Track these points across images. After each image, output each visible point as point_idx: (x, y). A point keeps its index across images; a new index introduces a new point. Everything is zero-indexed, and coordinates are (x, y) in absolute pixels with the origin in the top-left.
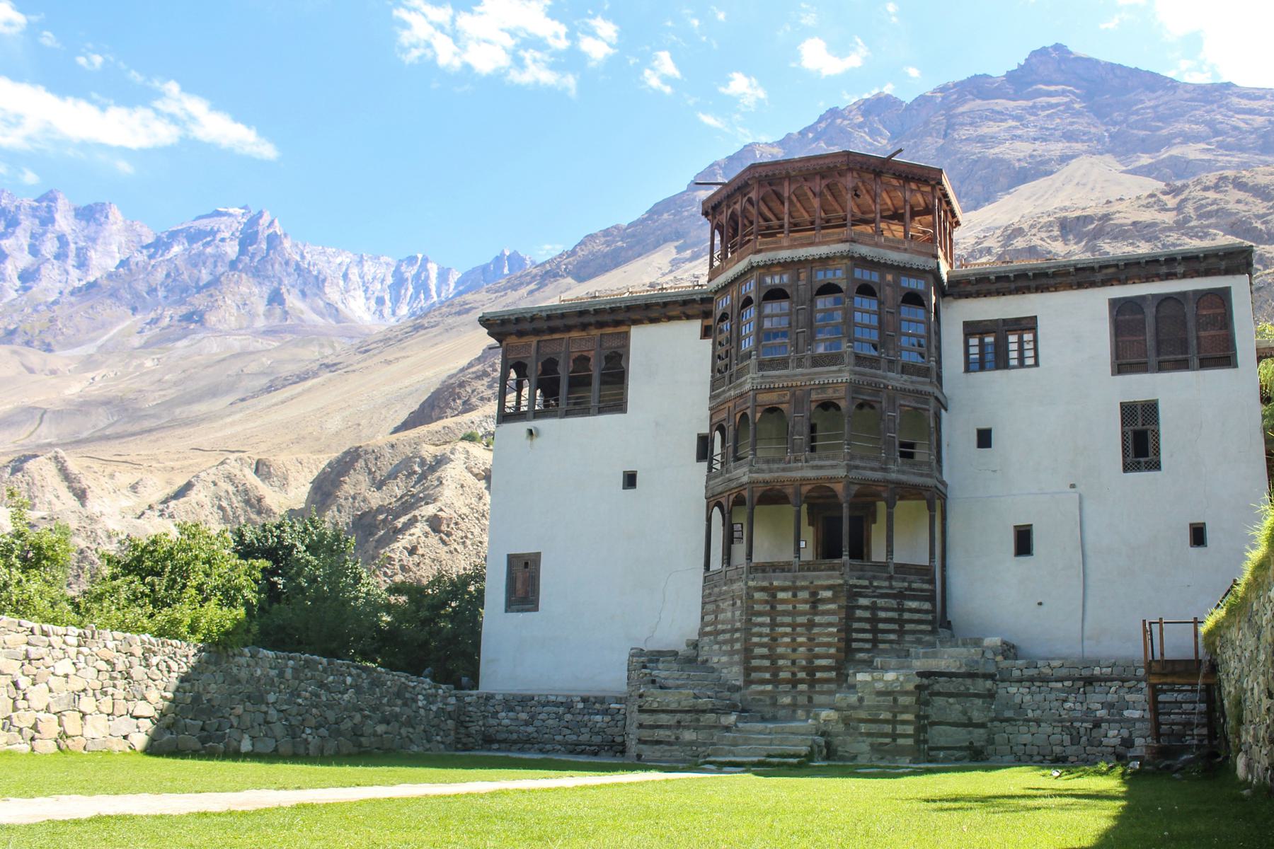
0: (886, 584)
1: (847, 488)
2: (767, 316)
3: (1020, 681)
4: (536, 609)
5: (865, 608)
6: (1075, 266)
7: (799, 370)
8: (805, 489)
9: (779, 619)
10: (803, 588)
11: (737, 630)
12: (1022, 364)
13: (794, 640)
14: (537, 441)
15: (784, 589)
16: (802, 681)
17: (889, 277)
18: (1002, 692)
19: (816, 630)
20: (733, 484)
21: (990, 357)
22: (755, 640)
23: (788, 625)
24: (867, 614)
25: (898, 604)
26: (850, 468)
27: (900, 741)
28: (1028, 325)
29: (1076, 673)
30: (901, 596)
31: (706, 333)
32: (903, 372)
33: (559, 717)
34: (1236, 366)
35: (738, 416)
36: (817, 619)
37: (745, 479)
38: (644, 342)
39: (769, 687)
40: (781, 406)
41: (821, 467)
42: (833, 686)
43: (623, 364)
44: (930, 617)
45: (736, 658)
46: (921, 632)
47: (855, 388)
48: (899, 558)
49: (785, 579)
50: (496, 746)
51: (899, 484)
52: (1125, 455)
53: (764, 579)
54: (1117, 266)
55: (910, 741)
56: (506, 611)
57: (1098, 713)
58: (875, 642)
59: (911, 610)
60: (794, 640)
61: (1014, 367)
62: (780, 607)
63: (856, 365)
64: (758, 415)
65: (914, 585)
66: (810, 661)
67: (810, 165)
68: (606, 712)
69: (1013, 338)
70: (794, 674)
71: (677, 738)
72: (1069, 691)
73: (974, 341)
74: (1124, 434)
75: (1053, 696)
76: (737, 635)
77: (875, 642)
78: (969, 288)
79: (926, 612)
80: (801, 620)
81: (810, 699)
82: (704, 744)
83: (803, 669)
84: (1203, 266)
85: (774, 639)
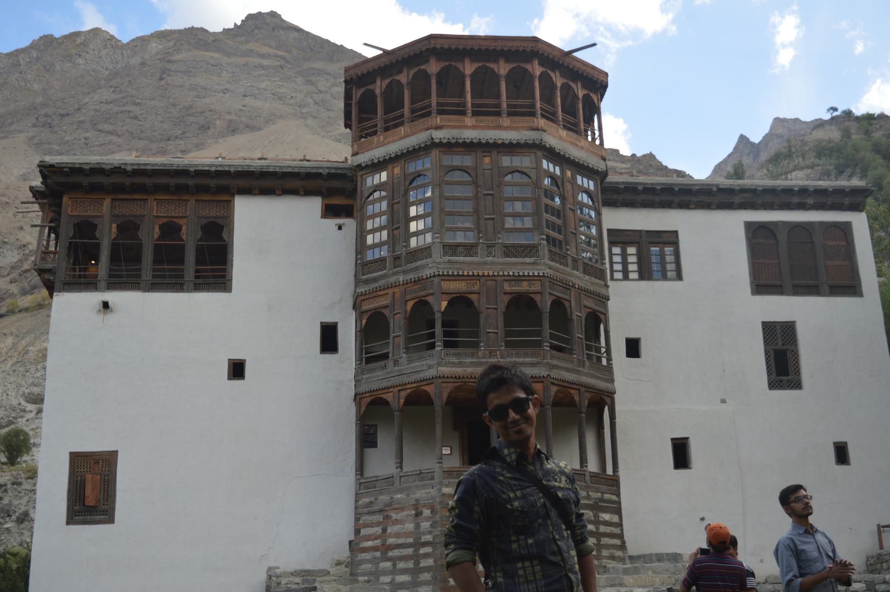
1: (546, 389)
2: (448, 199)
4: (111, 520)
6: (717, 186)
11: (425, 544)
12: (665, 278)
14: (111, 318)
20: (410, 379)
21: (633, 267)
25: (595, 516)
28: (670, 239)
31: (330, 211)
32: (584, 272)
34: (860, 295)
35: (410, 305)
37: (432, 373)
38: (250, 216)
40: (473, 297)
43: (225, 236)
44: (616, 531)
45: (426, 576)
46: (614, 546)
47: (553, 281)
51: (588, 387)
52: (769, 373)
56: (68, 523)
61: (657, 280)
64: (444, 304)
67: (499, 46)
69: (655, 249)
73: (616, 250)
74: (767, 352)
76: (428, 550)
78: (615, 197)
84: (829, 200)
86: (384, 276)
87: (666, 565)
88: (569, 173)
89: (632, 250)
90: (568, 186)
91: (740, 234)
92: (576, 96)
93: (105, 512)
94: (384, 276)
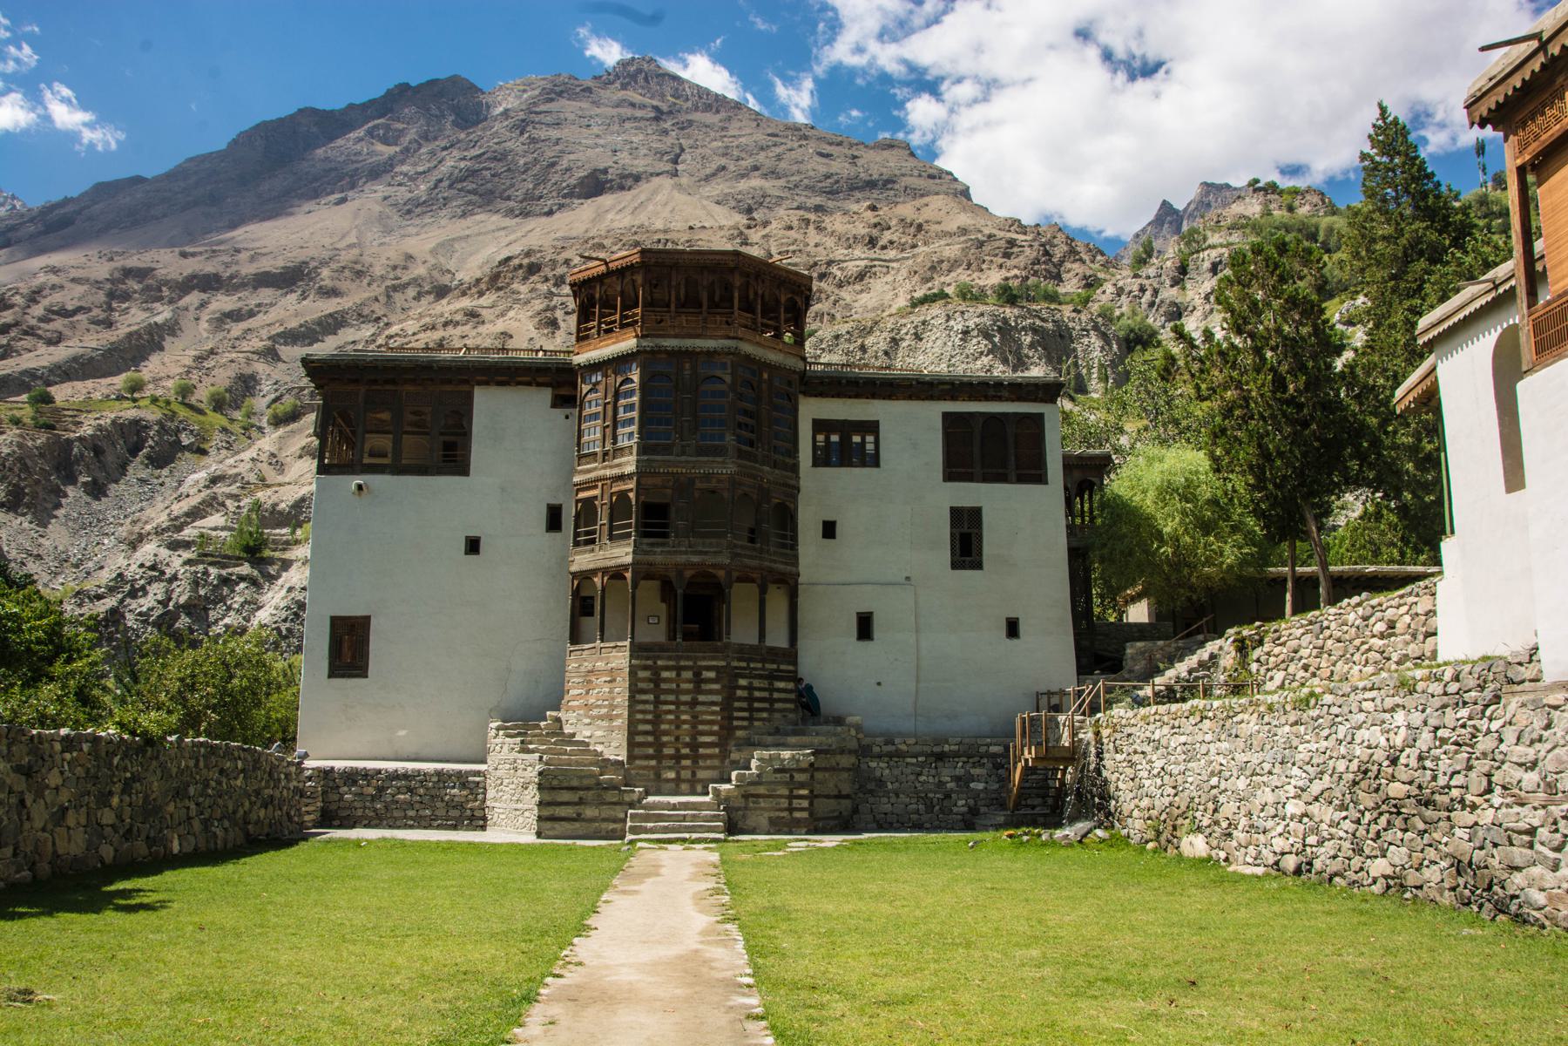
0: (759, 665)
3: (880, 756)
5: (743, 688)
7: (683, 458)
8: (688, 574)
9: (662, 697)
12: (863, 464)
13: (678, 717)
15: (667, 668)
18: (863, 766)
19: (699, 708)
22: (639, 716)
23: (671, 703)
27: (797, 815)
28: (872, 427)
29: (927, 749)
30: (772, 677)
33: (410, 790)
36: (701, 698)
38: (487, 404)
39: (653, 763)
41: (706, 553)
42: (716, 762)
48: (771, 641)
49: (669, 658)
50: (336, 823)
51: (771, 571)
53: (648, 658)
54: (952, 384)
55: (805, 815)
57: (949, 786)
59: (779, 690)
60: (678, 717)
63: (739, 457)
65: (783, 667)
66: (694, 738)
68: (464, 786)
70: (678, 750)
71: (579, 815)
72: (922, 765)
73: (820, 438)
75: (909, 771)
77: (750, 719)
79: (790, 691)
81: (694, 774)
82: (604, 820)
83: (687, 745)
86: (595, 469)
87: (830, 728)
88: (765, 376)
89: (835, 438)
90: (764, 386)
91: (938, 423)
92: (778, 301)
93: (360, 668)
94: (595, 469)
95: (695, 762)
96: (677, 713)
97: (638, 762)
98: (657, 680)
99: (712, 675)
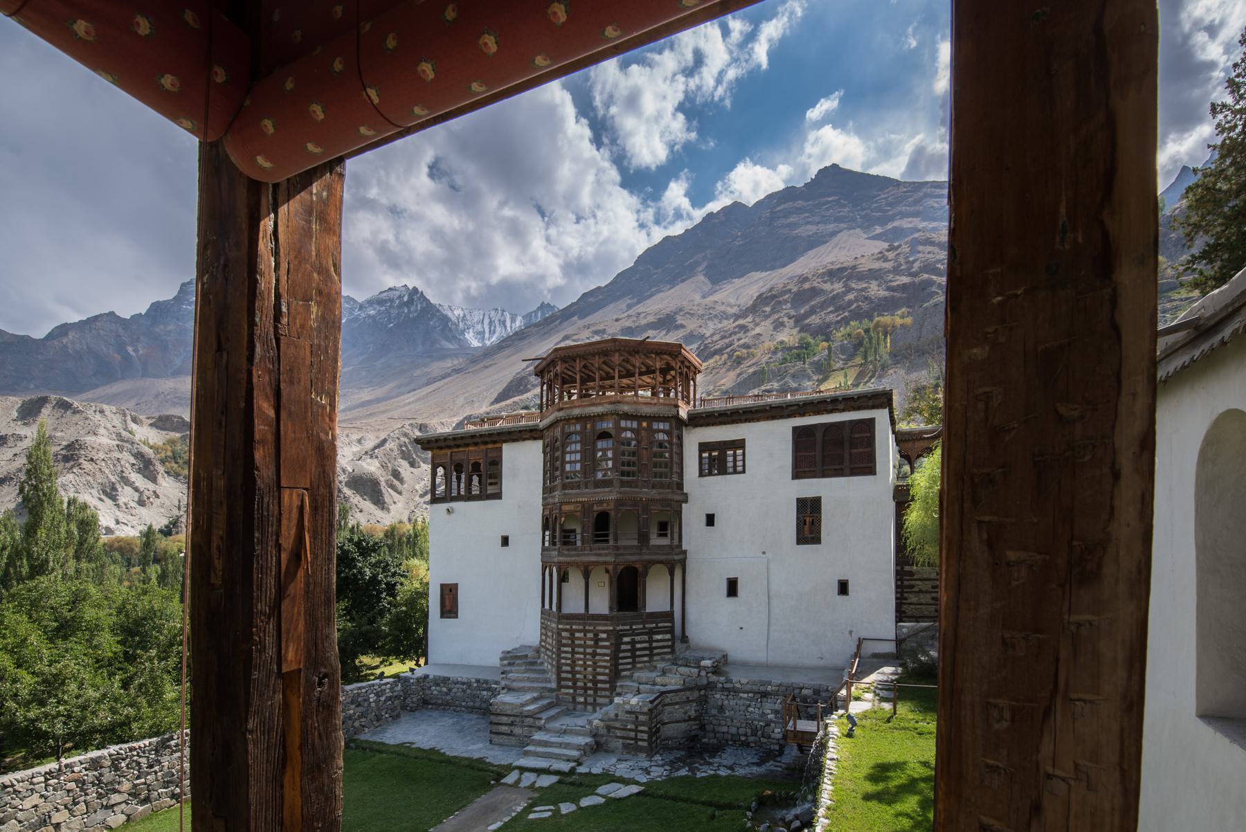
1: (615, 568)
5: (627, 643)
10: (590, 631)
15: (579, 631)
16: (590, 688)
17: (645, 424)
24: (629, 647)
26: (617, 555)
36: (599, 651)
58: (634, 663)
62: (577, 642)
66: (594, 677)
80: (589, 650)
83: (590, 681)
85: (574, 662)
88: (645, 424)
90: (643, 433)
95: (595, 692)
96: (585, 660)
97: (563, 690)
98: (573, 638)
99: (604, 636)
